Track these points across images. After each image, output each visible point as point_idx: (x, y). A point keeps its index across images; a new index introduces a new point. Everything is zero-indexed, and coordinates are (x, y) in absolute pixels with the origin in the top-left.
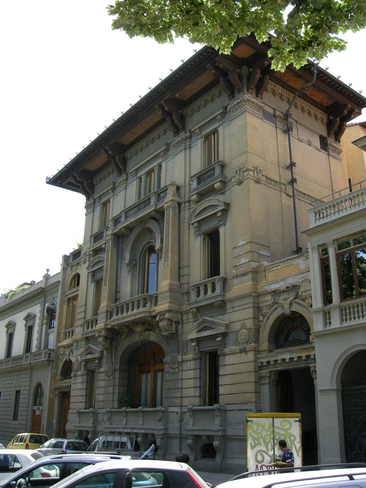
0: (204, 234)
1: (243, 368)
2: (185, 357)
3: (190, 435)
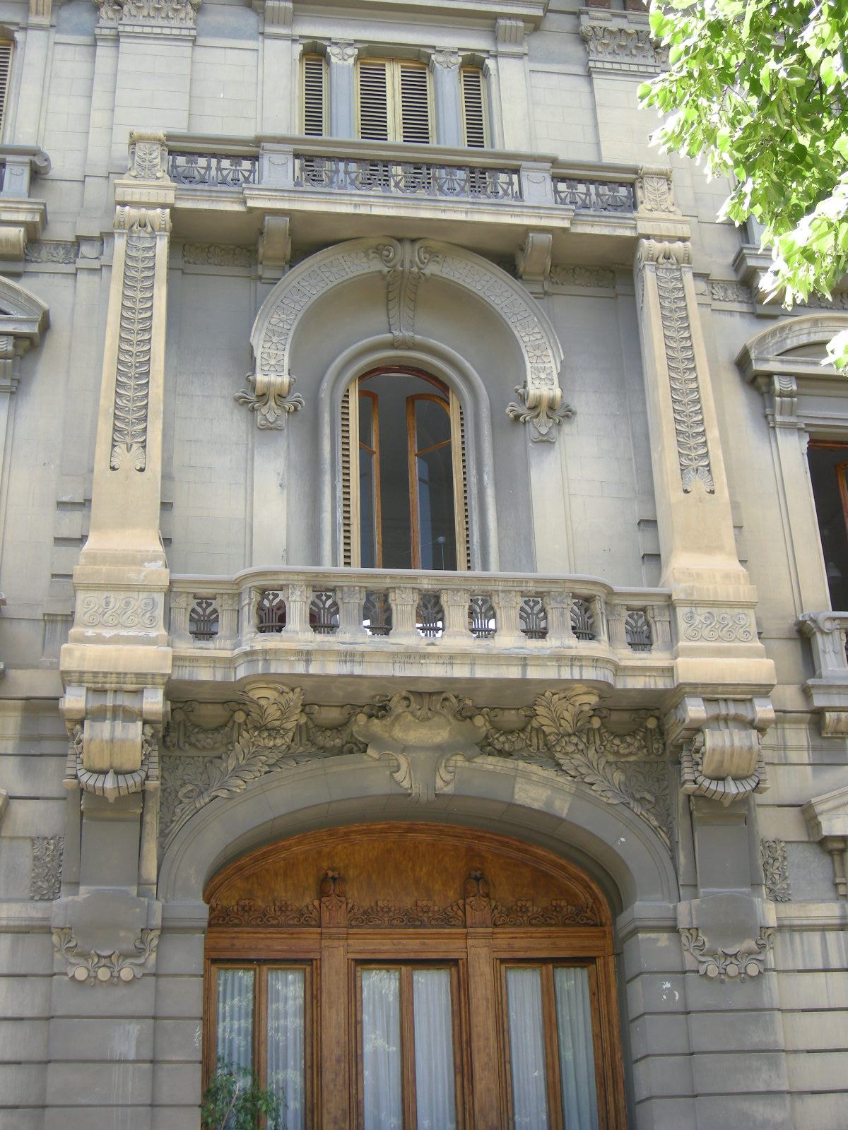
0: (811, 433)
2: (794, 912)
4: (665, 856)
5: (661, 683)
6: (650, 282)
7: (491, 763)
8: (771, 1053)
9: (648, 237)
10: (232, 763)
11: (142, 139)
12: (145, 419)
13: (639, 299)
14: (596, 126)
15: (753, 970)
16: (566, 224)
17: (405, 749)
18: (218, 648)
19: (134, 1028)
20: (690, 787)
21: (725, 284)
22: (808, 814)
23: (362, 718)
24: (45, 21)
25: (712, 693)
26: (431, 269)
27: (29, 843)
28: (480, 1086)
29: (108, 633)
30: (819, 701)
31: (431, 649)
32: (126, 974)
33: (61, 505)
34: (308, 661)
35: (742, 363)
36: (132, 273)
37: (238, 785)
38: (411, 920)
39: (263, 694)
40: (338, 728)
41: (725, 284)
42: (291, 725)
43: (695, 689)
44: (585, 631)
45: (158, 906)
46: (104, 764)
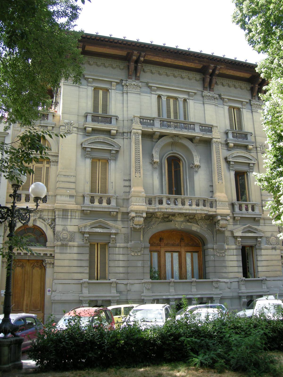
1: (274, 258)
2: (230, 247)
3: (244, 296)
4: (212, 238)
5: (214, 213)
6: (214, 146)
7: (189, 224)
8: (226, 267)
9: (214, 138)
10: (152, 223)
11: (136, 116)
12: (140, 168)
13: (212, 147)
14: (205, 114)
15: (224, 255)
16: (202, 136)
17: (177, 221)
18: (152, 206)
19: (140, 262)
20: (217, 229)
21: (223, 144)
22: (232, 232)
23: (171, 216)
24: (115, 88)
25: (221, 215)
26: (180, 141)
27: (123, 235)
28: (183, 270)
29: (137, 204)
30: (235, 216)
31: (184, 208)
32: (139, 254)
33: (124, 180)
34: (167, 209)
35: (226, 159)
36: (136, 142)
37: (154, 226)
38: (173, 245)
39: (159, 214)
40: (168, 217)
41: (223, 144)
42: (161, 217)
43: (219, 215)
44: (204, 205)
45: (143, 244)
46: (137, 224)
